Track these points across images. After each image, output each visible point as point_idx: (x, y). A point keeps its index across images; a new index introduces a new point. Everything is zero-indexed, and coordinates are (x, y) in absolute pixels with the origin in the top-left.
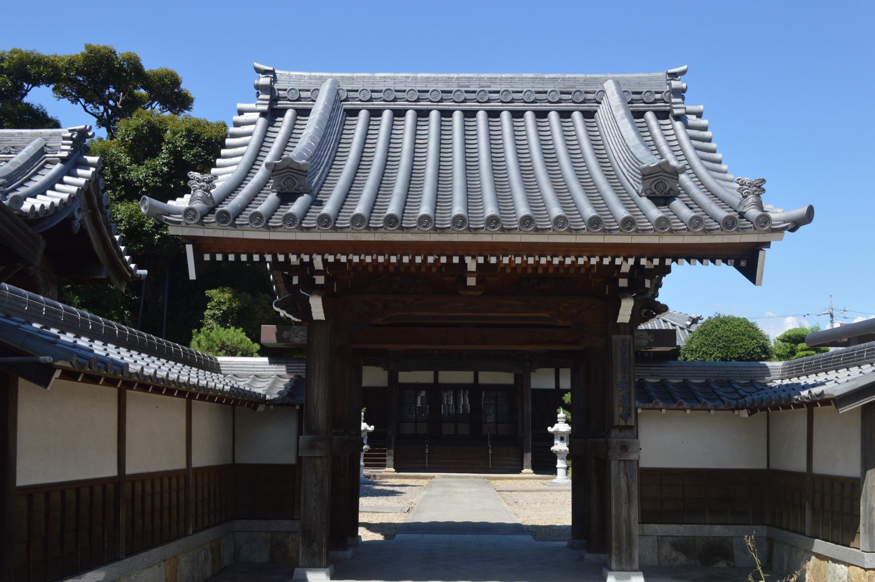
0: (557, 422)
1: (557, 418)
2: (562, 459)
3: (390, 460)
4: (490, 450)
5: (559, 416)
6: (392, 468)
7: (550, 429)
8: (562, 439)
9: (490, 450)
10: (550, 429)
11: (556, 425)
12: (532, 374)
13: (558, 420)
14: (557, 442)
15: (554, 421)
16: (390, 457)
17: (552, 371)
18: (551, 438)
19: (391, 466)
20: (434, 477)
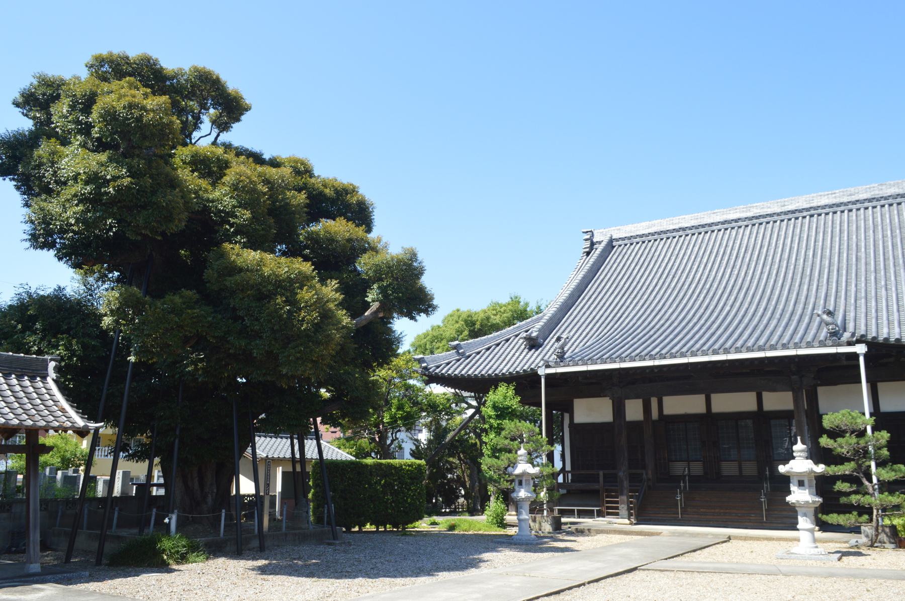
0: (794, 458)
1: (793, 452)
2: (805, 515)
3: (623, 509)
4: (763, 497)
5: (795, 448)
6: (627, 520)
7: (782, 469)
8: (801, 484)
9: (763, 497)
10: (782, 469)
11: (792, 462)
13: (795, 454)
14: (794, 488)
15: (789, 457)
16: (623, 506)
18: (784, 483)
19: (625, 517)
20: (658, 534)
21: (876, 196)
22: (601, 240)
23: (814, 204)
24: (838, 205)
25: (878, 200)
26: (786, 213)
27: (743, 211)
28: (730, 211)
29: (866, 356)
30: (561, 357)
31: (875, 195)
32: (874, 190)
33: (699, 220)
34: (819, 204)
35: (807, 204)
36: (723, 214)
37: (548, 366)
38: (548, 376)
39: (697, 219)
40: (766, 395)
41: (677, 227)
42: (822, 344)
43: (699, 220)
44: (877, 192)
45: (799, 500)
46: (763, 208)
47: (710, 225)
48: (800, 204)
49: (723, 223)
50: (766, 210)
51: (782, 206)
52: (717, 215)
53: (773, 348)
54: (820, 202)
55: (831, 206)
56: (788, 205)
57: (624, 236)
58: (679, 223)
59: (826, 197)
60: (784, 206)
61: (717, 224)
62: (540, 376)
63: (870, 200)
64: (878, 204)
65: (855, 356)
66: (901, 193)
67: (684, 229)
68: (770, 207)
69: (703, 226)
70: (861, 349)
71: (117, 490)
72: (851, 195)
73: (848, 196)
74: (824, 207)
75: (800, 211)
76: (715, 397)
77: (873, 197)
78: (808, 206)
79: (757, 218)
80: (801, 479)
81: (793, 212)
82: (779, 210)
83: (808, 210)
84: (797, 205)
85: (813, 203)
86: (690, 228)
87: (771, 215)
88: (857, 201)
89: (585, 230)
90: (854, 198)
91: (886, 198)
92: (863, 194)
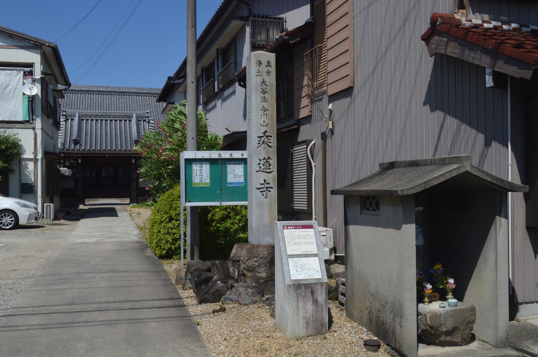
23: (130, 91)
24: (138, 93)
25: (150, 94)
26: (121, 92)
34: (132, 91)
47: (93, 91)
48: (125, 90)
49: (98, 91)
55: (135, 93)
58: (80, 88)
60: (120, 89)
61: (95, 91)
63: (148, 94)
64: (138, 95)
67: (82, 91)
69: (90, 91)
72: (142, 90)
74: (133, 93)
75: (126, 93)
78: (128, 91)
79: (111, 92)
81: (123, 92)
82: (118, 91)
83: (128, 93)
86: (85, 91)
87: (115, 92)
90: (143, 92)
91: (153, 94)
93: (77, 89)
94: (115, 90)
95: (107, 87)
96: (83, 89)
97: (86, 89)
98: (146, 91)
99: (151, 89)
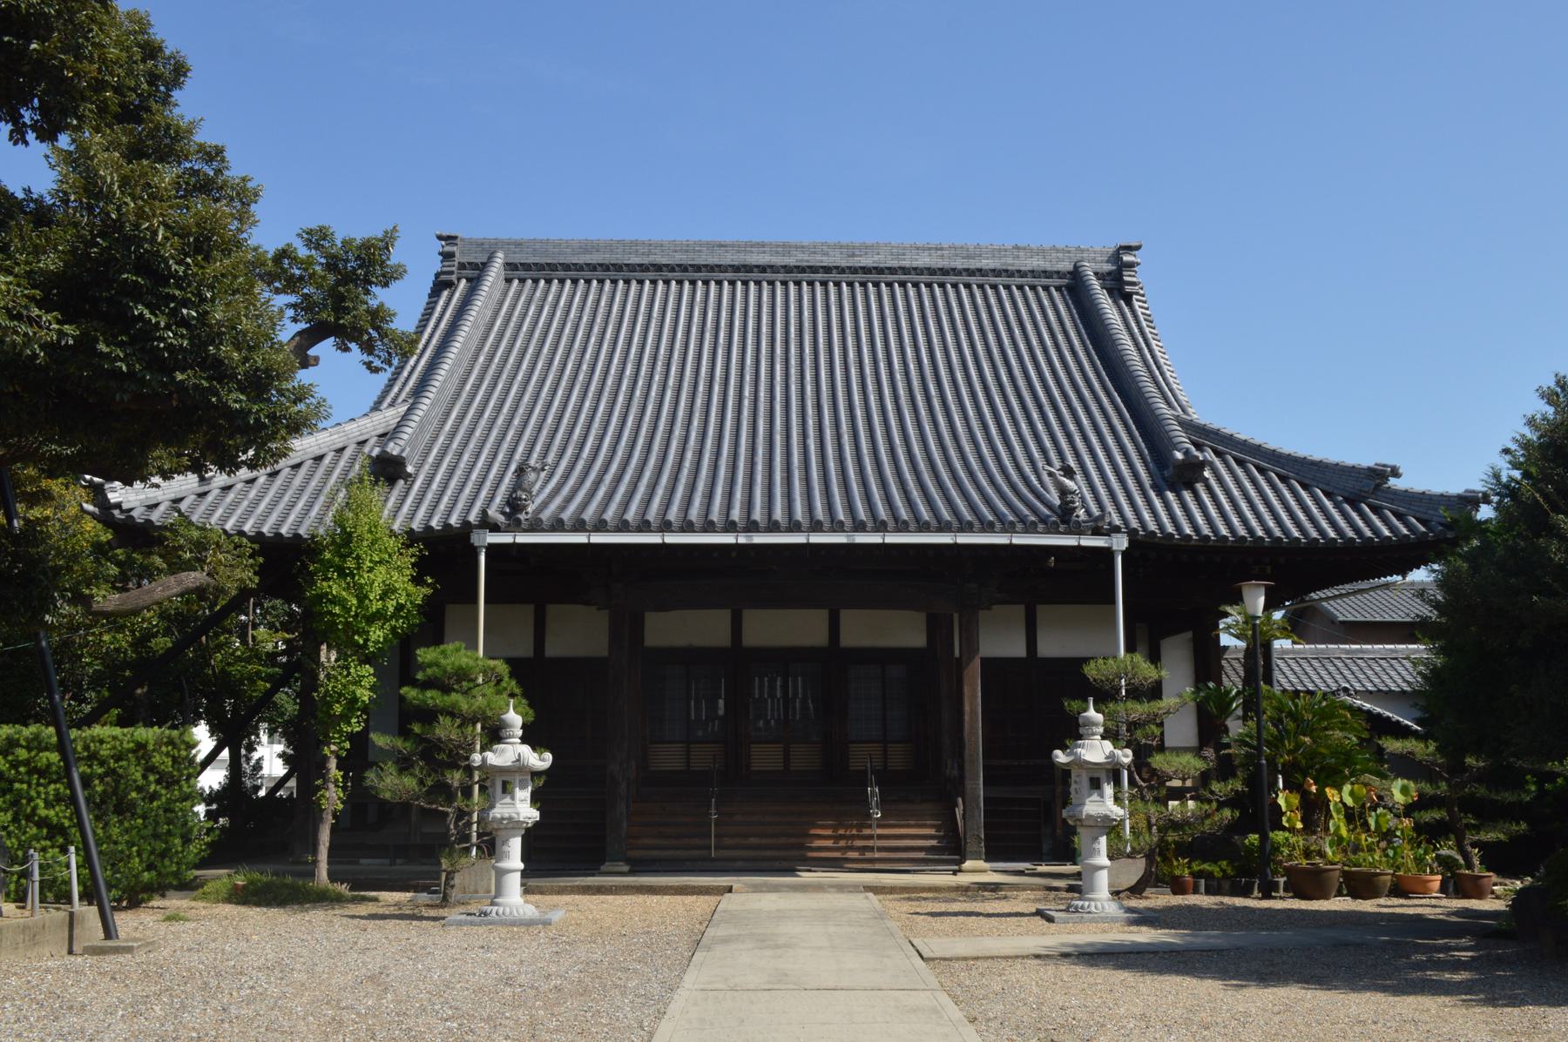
10: (1060, 757)
12: (982, 614)
13: (1082, 731)
15: (1072, 731)
17: (1019, 610)
21: (1010, 268)
22: (478, 261)
23: (907, 263)
24: (944, 272)
26: (854, 270)
27: (777, 252)
28: (752, 246)
29: (1126, 554)
30: (514, 505)
31: (802, 261)
32: (1005, 256)
33: (691, 255)
34: (915, 264)
35: (892, 259)
36: (738, 252)
37: (495, 528)
38: (492, 549)
39: (687, 251)
40: (846, 616)
41: (646, 261)
42: (1052, 529)
43: (691, 255)
44: (1010, 261)
45: (1093, 813)
46: (815, 253)
50: (818, 257)
51: (849, 256)
52: (727, 251)
53: (601, 526)
54: (917, 260)
56: (860, 256)
57: (530, 261)
59: (926, 253)
60: (853, 255)
62: (476, 548)
65: (1108, 553)
66: (1048, 269)
68: (827, 254)
70: (1120, 543)
71: (932, 832)
72: (968, 257)
73: (963, 258)
76: (846, 616)
77: (1005, 267)
78: (894, 263)
80: (1096, 775)
82: (844, 263)
84: (876, 258)
85: (904, 260)
88: (980, 270)
89: (445, 233)
90: (974, 264)
92: (988, 258)
93: (635, 260)
94: (827, 261)
95: (786, 248)
96: (664, 261)
97: (679, 258)
98: (987, 263)
99: (1017, 247)
